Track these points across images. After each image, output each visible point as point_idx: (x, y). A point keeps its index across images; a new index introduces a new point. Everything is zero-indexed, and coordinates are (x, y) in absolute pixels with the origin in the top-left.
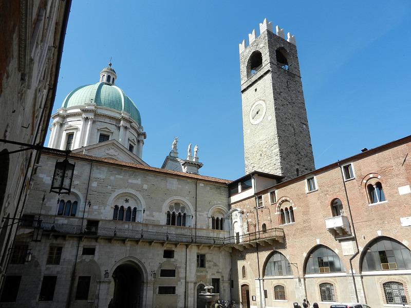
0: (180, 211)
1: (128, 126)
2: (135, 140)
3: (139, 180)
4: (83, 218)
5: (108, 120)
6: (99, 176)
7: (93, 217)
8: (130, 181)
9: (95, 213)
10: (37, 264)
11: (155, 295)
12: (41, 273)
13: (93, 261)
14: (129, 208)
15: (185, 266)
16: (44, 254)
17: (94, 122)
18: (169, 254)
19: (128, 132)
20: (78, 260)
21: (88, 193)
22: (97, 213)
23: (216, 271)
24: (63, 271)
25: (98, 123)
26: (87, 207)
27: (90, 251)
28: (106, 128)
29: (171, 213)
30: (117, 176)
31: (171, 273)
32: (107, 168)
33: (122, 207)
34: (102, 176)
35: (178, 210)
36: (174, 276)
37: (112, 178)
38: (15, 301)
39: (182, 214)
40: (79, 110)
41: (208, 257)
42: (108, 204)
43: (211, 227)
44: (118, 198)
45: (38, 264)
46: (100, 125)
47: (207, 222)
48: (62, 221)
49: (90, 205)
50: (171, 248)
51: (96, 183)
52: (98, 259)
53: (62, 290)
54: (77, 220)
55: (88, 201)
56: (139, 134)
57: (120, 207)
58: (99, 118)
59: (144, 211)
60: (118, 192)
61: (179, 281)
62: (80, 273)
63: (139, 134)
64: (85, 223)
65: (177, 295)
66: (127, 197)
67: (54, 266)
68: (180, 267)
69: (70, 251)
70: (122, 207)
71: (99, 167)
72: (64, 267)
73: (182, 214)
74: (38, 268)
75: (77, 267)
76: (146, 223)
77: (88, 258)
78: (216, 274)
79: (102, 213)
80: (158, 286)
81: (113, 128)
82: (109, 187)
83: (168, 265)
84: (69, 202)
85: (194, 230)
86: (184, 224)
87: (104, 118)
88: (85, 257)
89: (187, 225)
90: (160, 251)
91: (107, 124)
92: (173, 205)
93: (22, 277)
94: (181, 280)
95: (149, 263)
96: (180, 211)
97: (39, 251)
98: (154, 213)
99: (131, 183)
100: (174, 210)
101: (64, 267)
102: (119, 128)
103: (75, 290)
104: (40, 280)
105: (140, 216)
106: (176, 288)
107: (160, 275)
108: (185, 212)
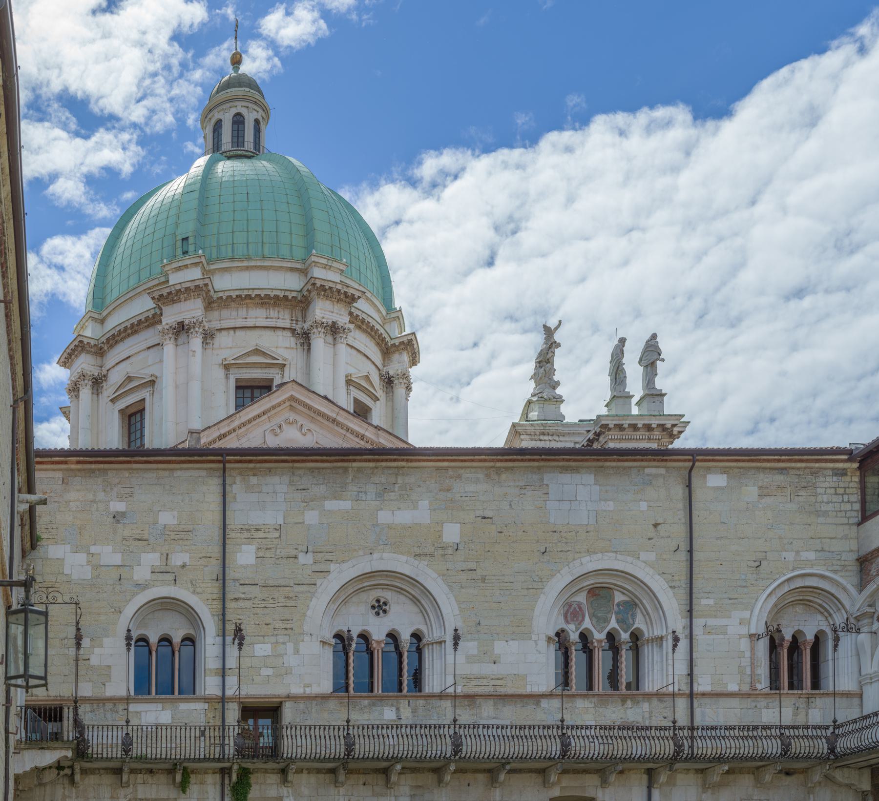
0: (613, 624)
4: (223, 700)
5: (258, 316)
7: (259, 688)
9: (266, 672)
21: (229, 596)
22: (270, 672)
26: (232, 651)
29: (574, 637)
35: (607, 621)
39: (625, 636)
42: (306, 628)
43: (763, 684)
47: (746, 661)
49: (242, 638)
51: (253, 548)
54: (202, 706)
55: (230, 628)
57: (355, 635)
59: (457, 639)
60: (342, 574)
64: (233, 714)
73: (625, 636)
82: (303, 559)
86: (636, 683)
87: (243, 312)
89: (652, 681)
91: (257, 332)
92: (582, 598)
96: (613, 624)
100: (587, 624)
105: (438, 665)
108: (639, 623)
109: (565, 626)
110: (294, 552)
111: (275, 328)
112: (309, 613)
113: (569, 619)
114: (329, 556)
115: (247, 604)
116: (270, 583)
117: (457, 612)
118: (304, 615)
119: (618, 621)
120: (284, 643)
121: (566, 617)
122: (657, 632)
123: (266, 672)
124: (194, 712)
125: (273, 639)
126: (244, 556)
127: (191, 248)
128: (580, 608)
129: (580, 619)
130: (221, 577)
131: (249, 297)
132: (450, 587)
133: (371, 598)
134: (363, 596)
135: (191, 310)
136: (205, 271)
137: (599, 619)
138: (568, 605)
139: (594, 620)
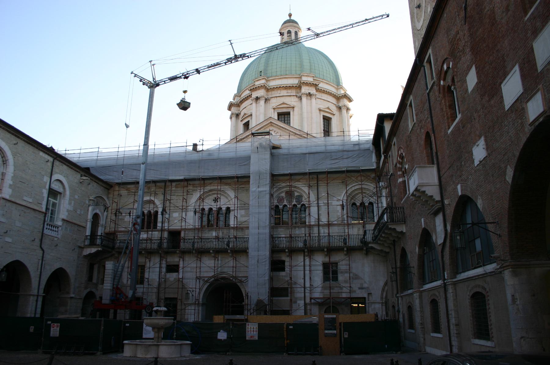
1: (313, 91)
2: (334, 109)
5: (284, 92)
14: (220, 209)
15: (303, 281)
17: (266, 100)
19: (313, 100)
23: (359, 286)
25: (273, 100)
28: (283, 103)
33: (211, 209)
40: (247, 92)
41: (343, 266)
46: (274, 102)
56: (338, 98)
58: (273, 92)
63: (338, 98)
64: (166, 235)
66: (215, 196)
69: (154, 270)
70: (211, 209)
77: (172, 276)
78: (358, 291)
81: (292, 101)
84: (149, 212)
85: (316, 229)
87: (279, 92)
88: (169, 275)
91: (284, 97)
94: (298, 302)
102: (300, 98)
111: (290, 96)
124: (156, 235)
127: (262, 74)
131: (280, 87)
134: (210, 197)
135: (261, 93)
136: (267, 81)
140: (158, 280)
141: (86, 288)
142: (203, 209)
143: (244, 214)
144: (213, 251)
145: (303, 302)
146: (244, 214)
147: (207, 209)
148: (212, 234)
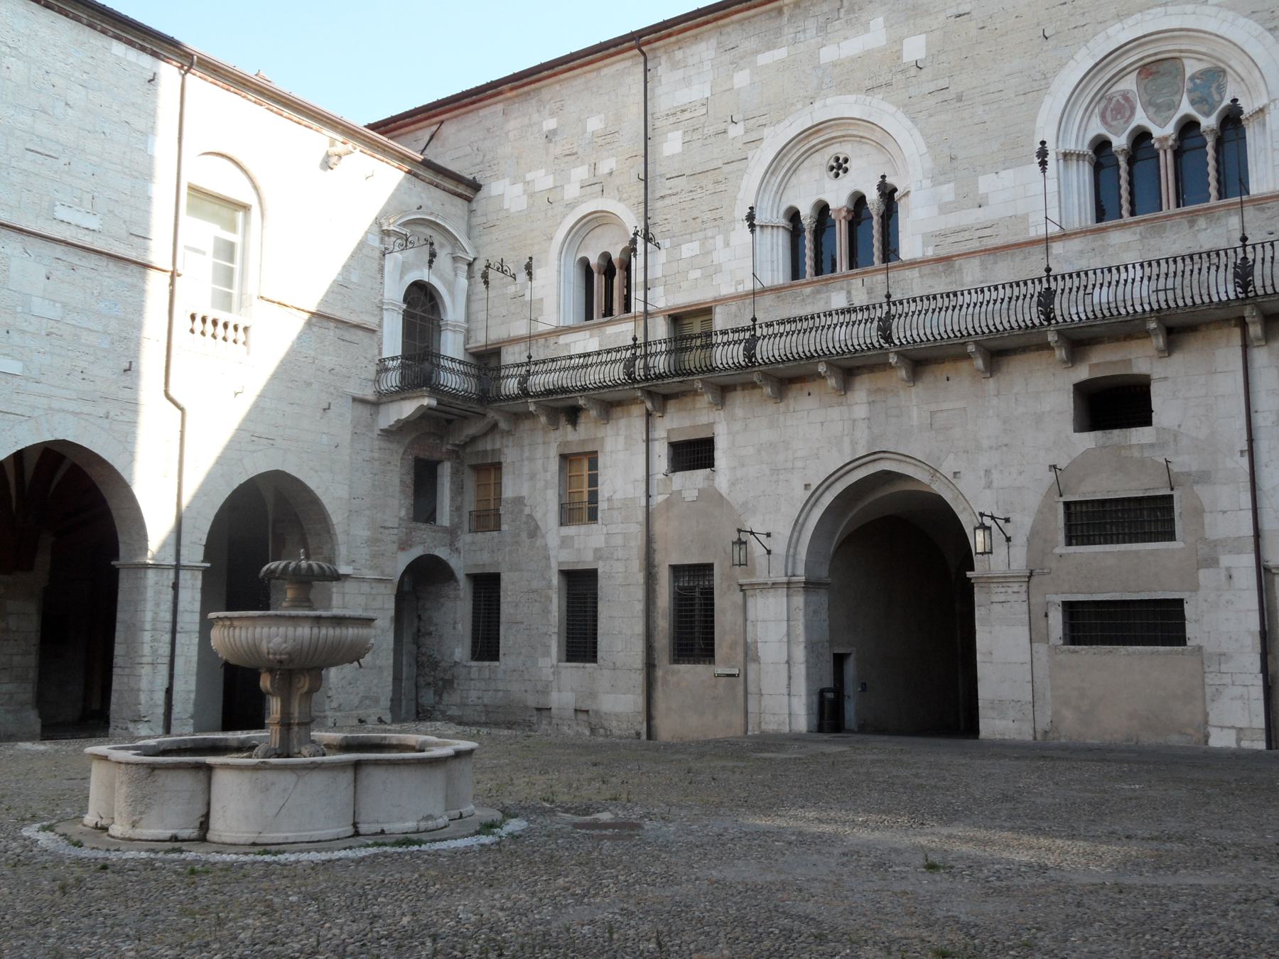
0: (1186, 108)
3: (878, 23)
6: (684, 96)
8: (828, 54)
10: (534, 531)
11: (1041, 649)
12: (548, 558)
13: (711, 497)
14: (859, 201)
15: (1245, 461)
16: (546, 488)
18: (1114, 405)
20: (658, 499)
22: (696, 274)
24: (610, 546)
27: (694, 454)
29: (1120, 142)
30: (764, 59)
31: (1147, 517)
32: (713, 42)
33: (823, 210)
34: (698, 91)
35: (1173, 106)
36: (1170, 536)
37: (742, 79)
38: (497, 659)
39: (1209, 122)
44: (793, 170)
45: (537, 527)
48: (586, 342)
50: (1128, 362)
51: (680, 132)
52: (733, 484)
53: (621, 621)
61: (1212, 562)
62: (670, 556)
64: (660, 329)
65: (1200, 648)
67: (583, 529)
68: (1204, 477)
70: (823, 210)
71: (679, 55)
72: (613, 529)
73: (1209, 122)
74: (539, 542)
75: (659, 527)
76: (943, 252)
79: (718, 270)
80: (1060, 598)
83: (1117, 465)
88: (680, 478)
90: (1048, 391)
93: (503, 576)
94: (1226, 560)
95: (987, 472)
97: (533, 477)
98: (986, 183)
99: (834, 65)
100: (1141, 118)
101: (613, 529)
103: (663, 624)
104: (550, 588)
106: (1188, 610)
107: (1061, 536)
109: (1103, 131)
110: (722, 127)
112: (740, 195)
113: (1109, 119)
114: (762, 121)
115: (674, 199)
116: (699, 170)
117: (924, 149)
118: (735, 198)
119: (1193, 103)
120: (713, 237)
121: (1103, 117)
122: (1258, 105)
123: (696, 274)
125: (701, 235)
126: (671, 145)
128: (1127, 99)
129: (1127, 114)
130: (642, 176)
132: (913, 120)
133: (827, 158)
137: (1158, 108)
138: (1102, 96)
139: (1151, 110)
140: (643, 502)
141: (404, 546)
142: (794, 216)
143: (951, 197)
144: (830, 364)
145: (1250, 559)
146: (951, 197)
147: (806, 212)
148: (828, 302)
